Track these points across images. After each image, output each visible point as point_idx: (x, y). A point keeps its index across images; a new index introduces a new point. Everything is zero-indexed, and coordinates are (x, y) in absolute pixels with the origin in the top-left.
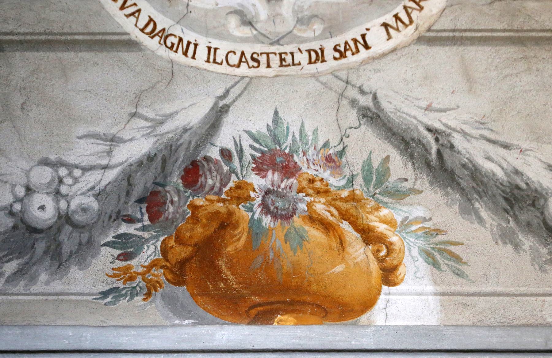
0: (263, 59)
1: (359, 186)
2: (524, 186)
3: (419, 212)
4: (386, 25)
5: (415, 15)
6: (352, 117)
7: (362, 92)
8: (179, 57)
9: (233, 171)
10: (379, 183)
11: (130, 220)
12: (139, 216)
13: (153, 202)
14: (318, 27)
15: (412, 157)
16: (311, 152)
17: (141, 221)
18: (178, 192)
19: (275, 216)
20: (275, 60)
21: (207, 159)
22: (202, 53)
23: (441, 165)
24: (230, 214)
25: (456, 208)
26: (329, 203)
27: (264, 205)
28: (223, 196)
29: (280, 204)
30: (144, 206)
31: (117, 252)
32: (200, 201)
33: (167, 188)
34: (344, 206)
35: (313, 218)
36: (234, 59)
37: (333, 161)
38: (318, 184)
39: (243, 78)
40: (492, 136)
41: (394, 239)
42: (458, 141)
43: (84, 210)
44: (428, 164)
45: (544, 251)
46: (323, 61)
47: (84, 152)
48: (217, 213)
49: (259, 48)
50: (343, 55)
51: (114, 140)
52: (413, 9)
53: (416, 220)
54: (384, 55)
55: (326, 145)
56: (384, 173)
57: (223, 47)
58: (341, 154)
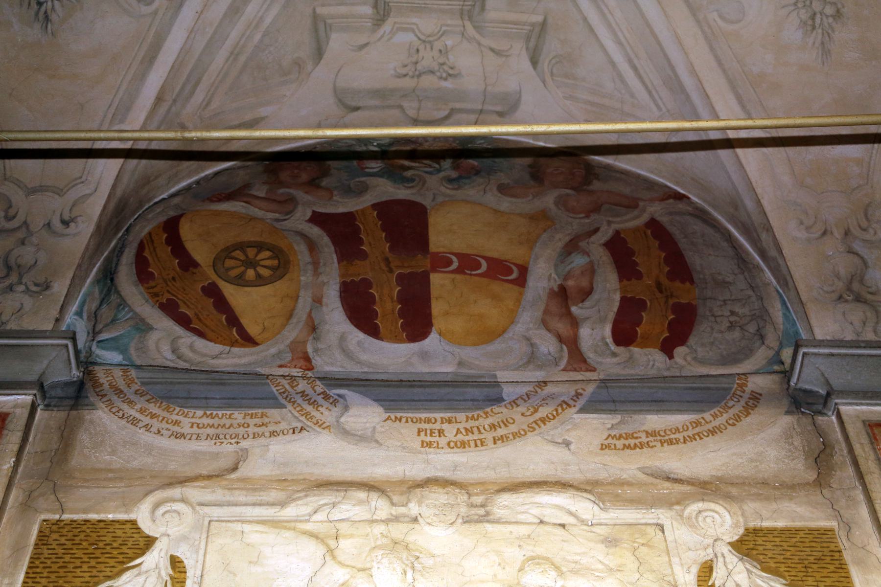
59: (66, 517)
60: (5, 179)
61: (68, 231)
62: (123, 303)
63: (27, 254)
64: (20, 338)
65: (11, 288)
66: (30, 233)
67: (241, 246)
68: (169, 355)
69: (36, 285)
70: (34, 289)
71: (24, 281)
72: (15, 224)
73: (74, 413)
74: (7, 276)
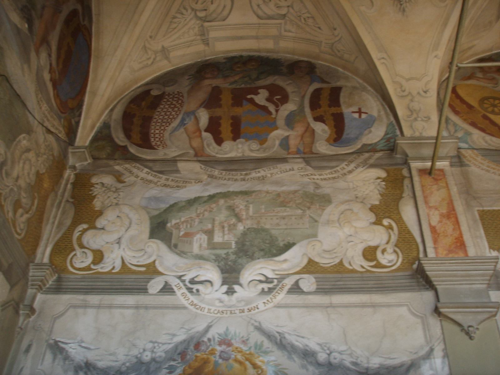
0: (225, 312)
1: (253, 350)
2: (309, 350)
3: (273, 358)
4: (264, 303)
5: (274, 300)
6: (251, 328)
7: (256, 321)
8: (199, 311)
9: (211, 345)
10: (260, 349)
11: (174, 360)
12: (177, 359)
13: (183, 355)
14: (243, 303)
15: (271, 341)
16: (237, 339)
17: (177, 360)
18: (192, 351)
19: (224, 359)
20: (229, 312)
21: (203, 341)
22: (206, 310)
23: (282, 344)
24: (208, 358)
25: (286, 357)
26: (242, 355)
27: (220, 357)
28: (207, 353)
29: (225, 355)
30: (180, 356)
31: (168, 371)
32: (198, 354)
33: (189, 350)
34: (247, 356)
35: (236, 360)
36: (216, 312)
37: (244, 342)
38: (239, 349)
39: (218, 317)
40: (298, 334)
41: (264, 367)
42: (287, 336)
43: (160, 357)
44: (276, 343)
45: (317, 371)
46: (244, 312)
47: (164, 338)
48: (203, 359)
49: (224, 309)
50: (250, 311)
51: (174, 335)
52: (273, 298)
53: (272, 361)
54: (263, 311)
55: (242, 337)
56: (262, 345)
57: (213, 309)
58: (247, 340)
59: (485, 208)
60: (397, 75)
61: (427, 95)
62: (455, 125)
63: (415, 105)
64: (429, 140)
65: (416, 119)
66: (413, 97)
67: (487, 98)
68: (484, 144)
69: (425, 117)
70: (425, 119)
71: (420, 116)
72: (405, 93)
73: (462, 168)
74: (412, 114)
